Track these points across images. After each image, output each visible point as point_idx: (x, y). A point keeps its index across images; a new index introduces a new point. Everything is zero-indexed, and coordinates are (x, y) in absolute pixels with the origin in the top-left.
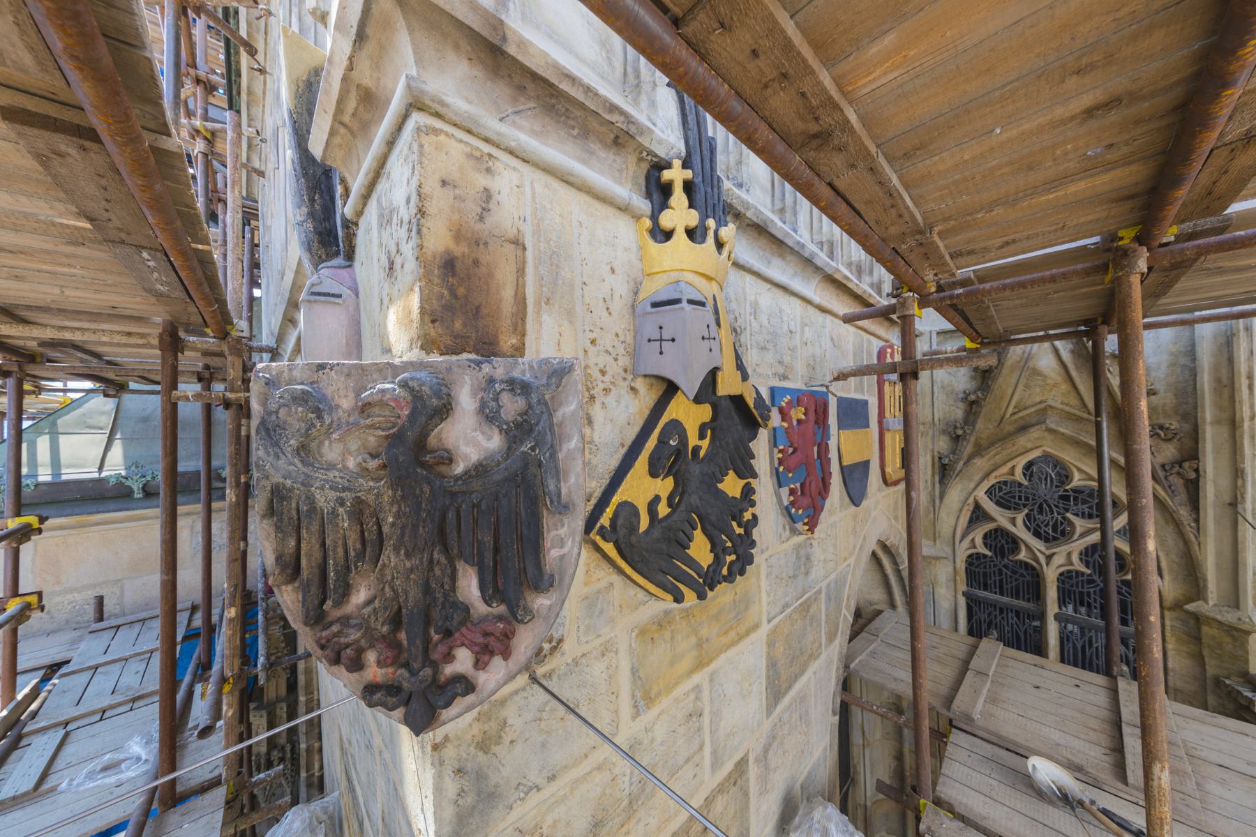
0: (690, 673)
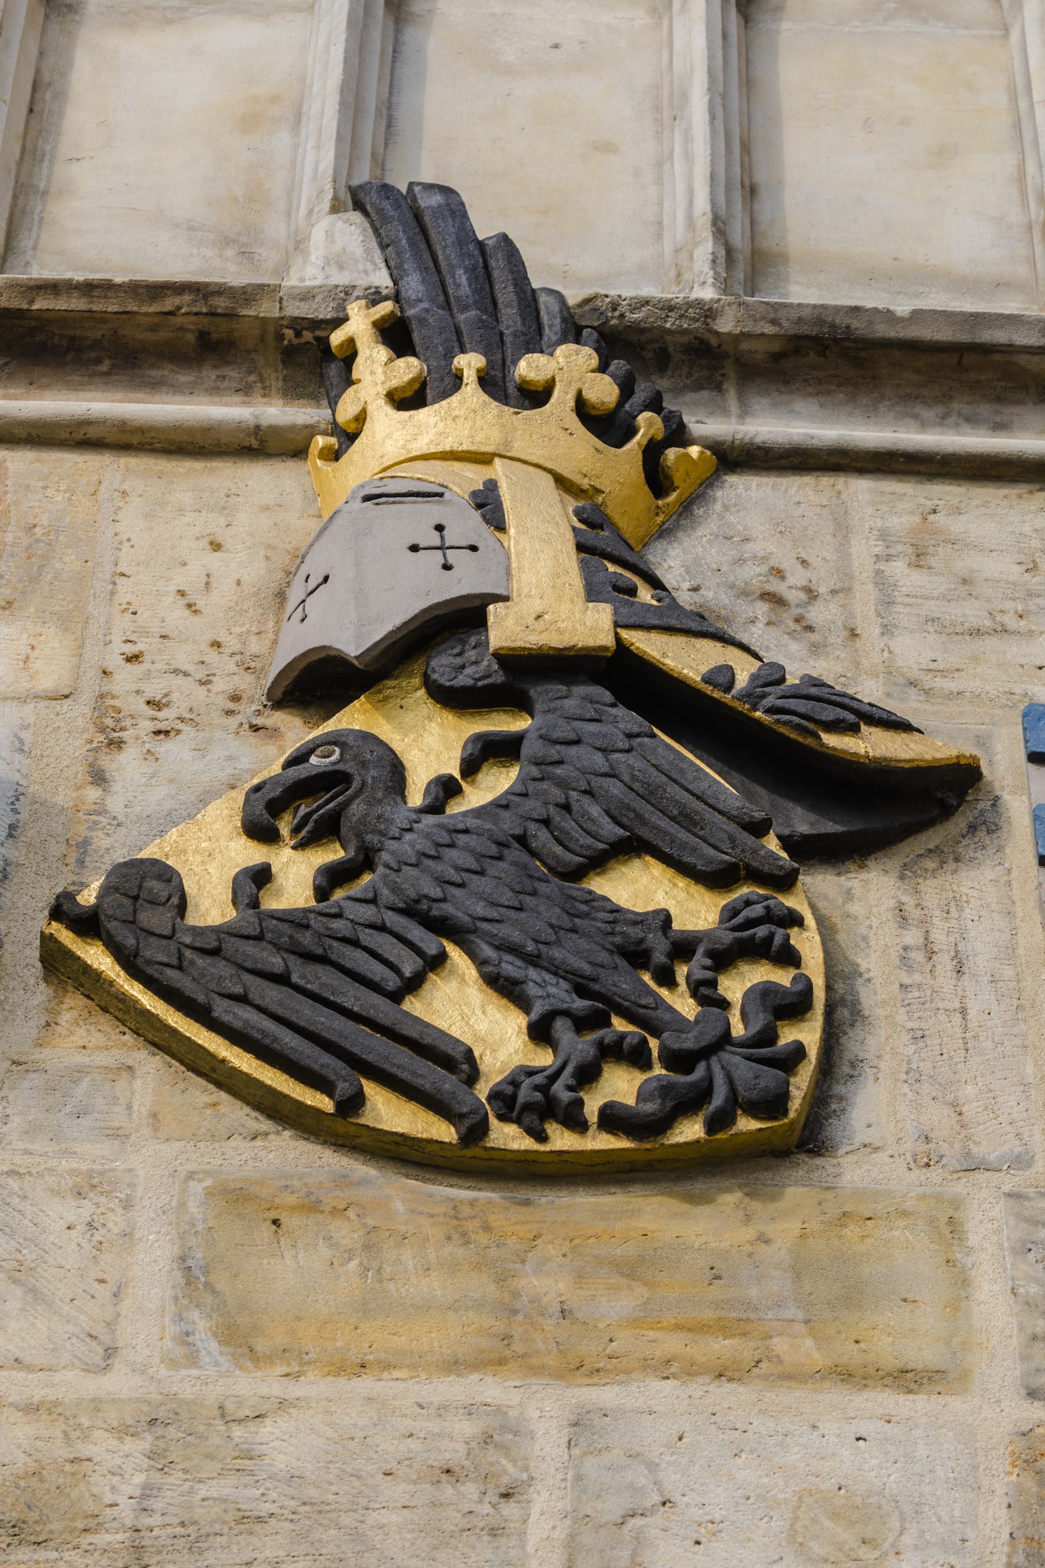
0: (454, 1366)
